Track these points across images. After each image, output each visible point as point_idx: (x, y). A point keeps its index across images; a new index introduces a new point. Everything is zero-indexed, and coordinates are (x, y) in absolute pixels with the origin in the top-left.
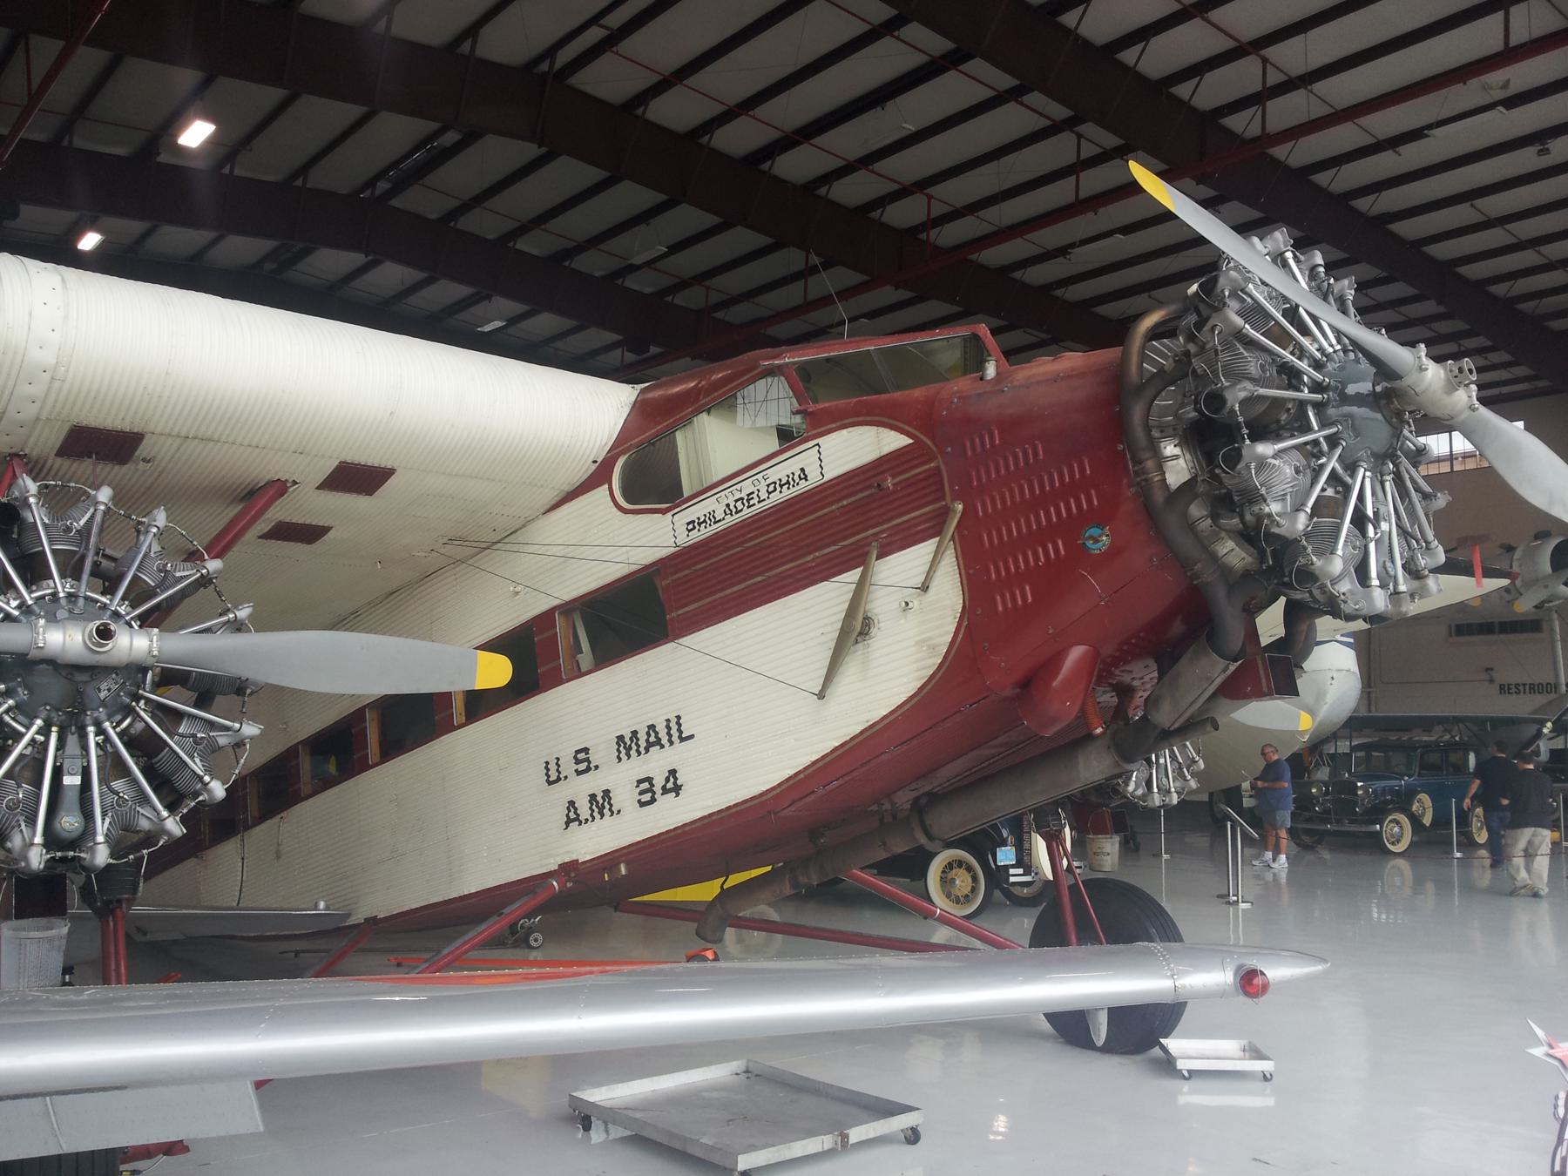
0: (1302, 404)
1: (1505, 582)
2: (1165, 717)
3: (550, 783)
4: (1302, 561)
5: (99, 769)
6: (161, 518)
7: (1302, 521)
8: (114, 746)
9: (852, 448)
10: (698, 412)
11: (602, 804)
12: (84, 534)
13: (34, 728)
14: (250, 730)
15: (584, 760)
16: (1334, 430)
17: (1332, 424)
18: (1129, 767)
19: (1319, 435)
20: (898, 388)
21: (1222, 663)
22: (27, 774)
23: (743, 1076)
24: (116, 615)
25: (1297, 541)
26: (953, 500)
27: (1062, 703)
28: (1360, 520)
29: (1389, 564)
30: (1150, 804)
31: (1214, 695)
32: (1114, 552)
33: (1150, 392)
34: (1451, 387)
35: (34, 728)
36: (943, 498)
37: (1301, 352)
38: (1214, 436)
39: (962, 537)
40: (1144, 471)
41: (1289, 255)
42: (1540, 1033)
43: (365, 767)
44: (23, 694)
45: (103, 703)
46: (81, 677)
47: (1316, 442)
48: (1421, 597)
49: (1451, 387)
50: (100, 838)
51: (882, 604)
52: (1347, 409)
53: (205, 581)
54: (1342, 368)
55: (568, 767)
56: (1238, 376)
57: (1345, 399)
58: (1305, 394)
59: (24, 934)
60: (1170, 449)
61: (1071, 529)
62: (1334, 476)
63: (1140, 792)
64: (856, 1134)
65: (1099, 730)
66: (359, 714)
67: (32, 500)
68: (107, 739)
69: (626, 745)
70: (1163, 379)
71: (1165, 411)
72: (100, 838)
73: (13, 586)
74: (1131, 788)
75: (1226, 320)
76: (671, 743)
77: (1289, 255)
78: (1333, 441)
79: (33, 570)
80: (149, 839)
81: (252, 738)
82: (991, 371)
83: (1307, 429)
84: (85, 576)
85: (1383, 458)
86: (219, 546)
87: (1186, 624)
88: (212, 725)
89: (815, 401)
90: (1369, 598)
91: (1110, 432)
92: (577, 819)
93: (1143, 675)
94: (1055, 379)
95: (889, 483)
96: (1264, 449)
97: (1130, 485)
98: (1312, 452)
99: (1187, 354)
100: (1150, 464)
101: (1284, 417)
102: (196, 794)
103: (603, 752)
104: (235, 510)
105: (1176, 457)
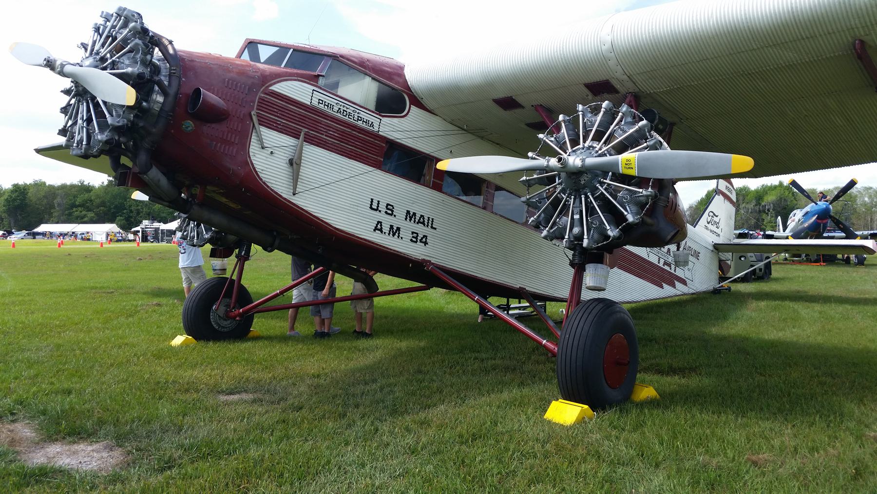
3: (371, 208)
11: (395, 231)
15: (390, 210)
55: (382, 207)
69: (410, 216)
92: (381, 230)
103: (400, 213)
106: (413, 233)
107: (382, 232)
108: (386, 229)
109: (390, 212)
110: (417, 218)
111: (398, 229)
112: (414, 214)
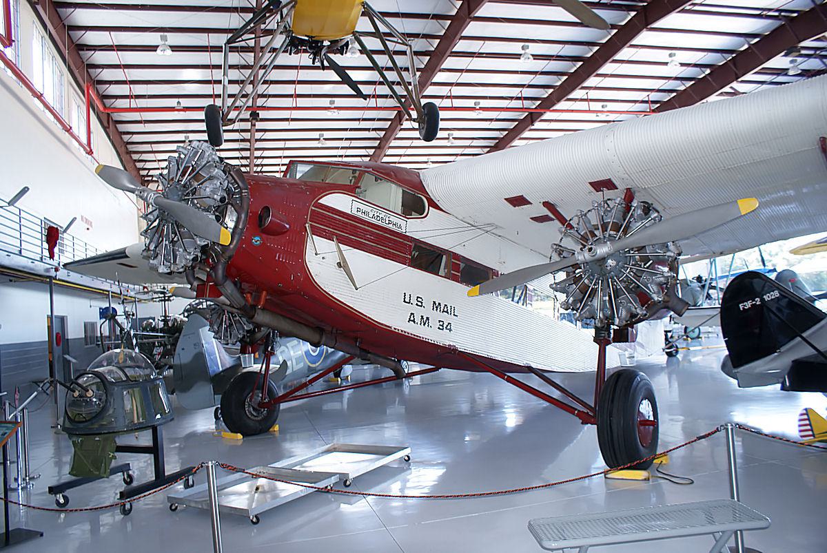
3: (405, 301)
11: (425, 321)
55: (414, 301)
69: (436, 306)
103: (428, 304)
106: (440, 321)
107: (414, 322)
108: (418, 319)
109: (419, 304)
110: (442, 306)
111: (428, 318)
112: (439, 304)
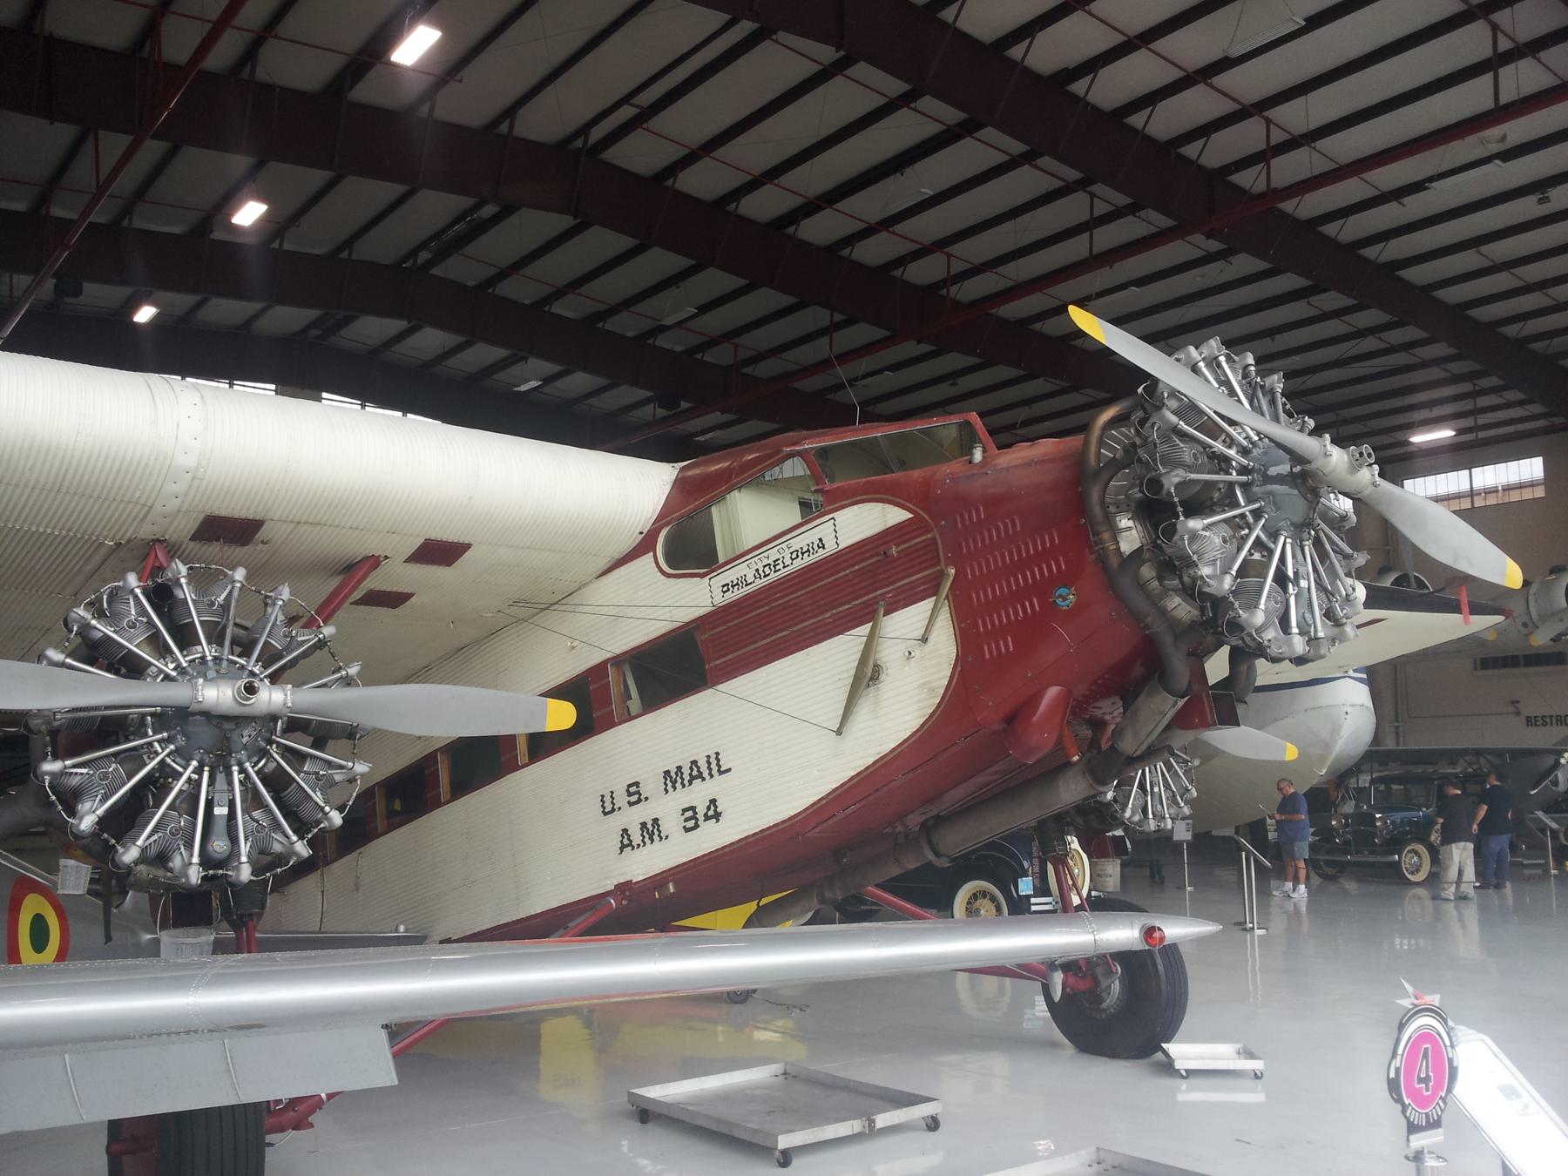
0: (1231, 485)
1: (1499, 618)
2: (1128, 745)
3: (606, 814)
4: (1232, 614)
5: (242, 802)
6: (285, 593)
7: (1228, 582)
8: (254, 784)
9: (861, 522)
10: (730, 490)
11: (652, 830)
12: (225, 607)
13: (191, 769)
14: (361, 768)
16: (1257, 505)
17: (1256, 501)
18: (1102, 789)
19: (1246, 510)
20: (903, 465)
21: (1171, 699)
22: (184, 806)
23: (781, 1078)
24: (252, 674)
25: (1225, 598)
26: (947, 565)
27: (1041, 735)
28: (1281, 579)
29: (1308, 616)
30: (1145, 828)
31: (1168, 727)
32: (1079, 607)
33: (1105, 477)
34: (1355, 467)
35: (191, 769)
36: (938, 563)
37: (1231, 442)
38: (1157, 512)
39: (954, 596)
40: (1101, 542)
41: (1222, 359)
42: (1409, 988)
43: (437, 804)
44: (181, 741)
45: (245, 747)
46: (228, 726)
47: (1243, 516)
48: (1341, 641)
49: (1355, 467)
50: (244, 859)
51: (889, 655)
52: (1269, 487)
53: (321, 644)
54: (1265, 453)
55: (622, 799)
56: (1174, 463)
57: (1267, 479)
58: (1234, 476)
59: (180, 940)
60: (1124, 522)
61: (1044, 589)
62: (1258, 543)
63: (1136, 818)
64: (882, 1120)
65: (1076, 758)
66: (431, 758)
67: (183, 580)
68: (248, 777)
69: (672, 779)
70: (1115, 466)
71: (1119, 491)
72: (244, 859)
73: (172, 653)
74: (1128, 814)
75: (1163, 418)
76: (711, 776)
77: (1222, 359)
78: (1257, 514)
79: (186, 638)
80: (280, 859)
81: (362, 775)
82: (978, 455)
83: (1236, 505)
84: (227, 643)
85: (1300, 528)
86: (327, 610)
87: (1141, 667)
88: (329, 764)
89: (832, 480)
90: (1290, 644)
91: (1072, 509)
92: (630, 844)
93: (1110, 709)
94: (1029, 464)
95: (894, 550)
96: (1195, 524)
97: (1092, 552)
98: (1237, 524)
99: (1134, 445)
100: (1106, 536)
101: (1216, 495)
102: (319, 822)
103: (652, 785)
104: (335, 582)
105: (1130, 529)
